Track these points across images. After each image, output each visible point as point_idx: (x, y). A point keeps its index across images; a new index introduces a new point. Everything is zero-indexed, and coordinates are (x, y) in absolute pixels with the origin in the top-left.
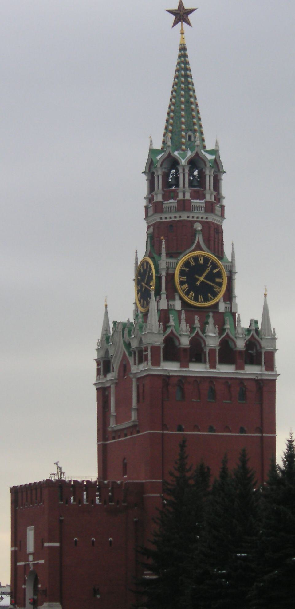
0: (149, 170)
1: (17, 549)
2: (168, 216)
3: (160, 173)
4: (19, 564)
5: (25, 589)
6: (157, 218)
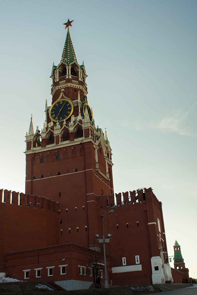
0: (59, 68)
2: (74, 85)
3: (70, 68)
6: (69, 85)
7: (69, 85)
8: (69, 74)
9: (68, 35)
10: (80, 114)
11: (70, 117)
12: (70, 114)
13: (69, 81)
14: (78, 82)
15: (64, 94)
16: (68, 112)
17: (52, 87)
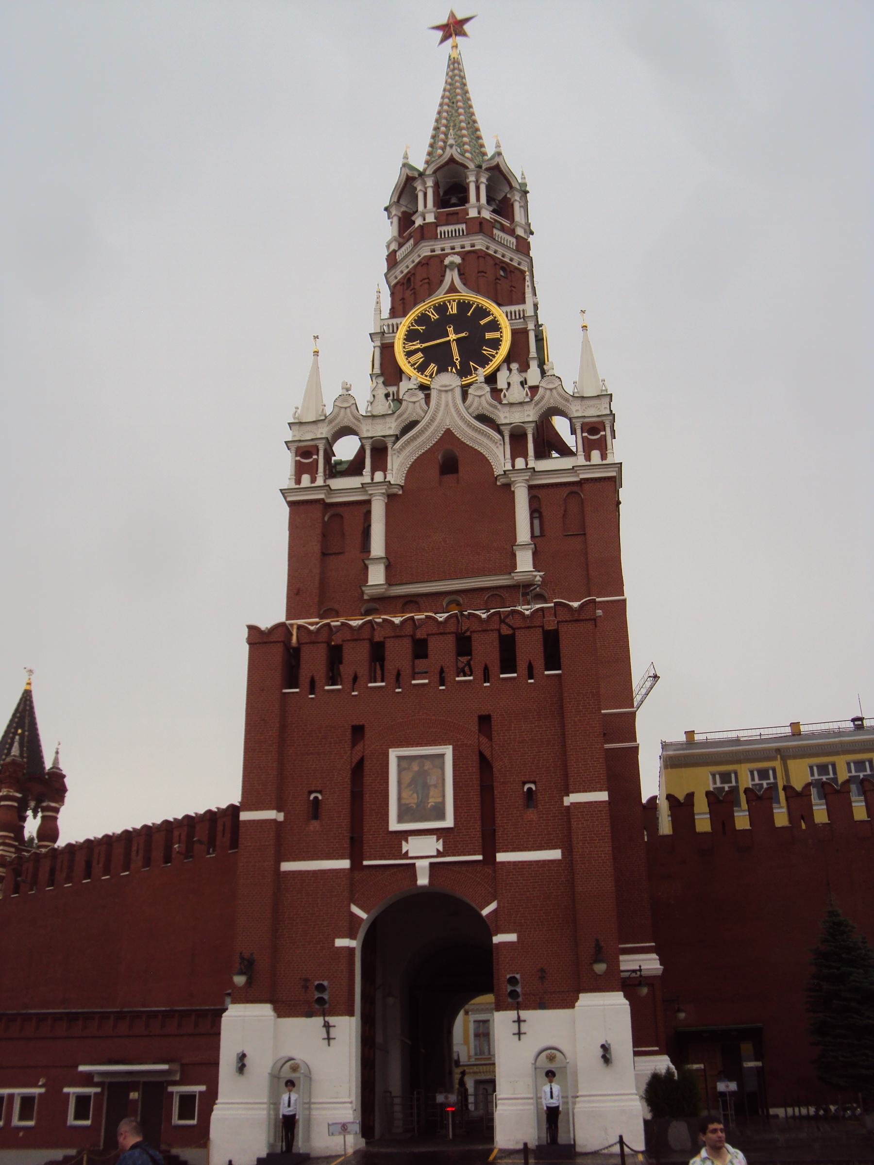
0: (435, 172)
1: (280, 817)
2: (501, 250)
3: (483, 180)
4: (287, 866)
5: (351, 951)
6: (480, 243)
7: (480, 243)
8: (478, 199)
9: (455, 65)
10: (534, 365)
11: (498, 369)
12: (494, 357)
13: (481, 227)
14: (514, 240)
15: (461, 274)
16: (487, 351)
17: (394, 246)
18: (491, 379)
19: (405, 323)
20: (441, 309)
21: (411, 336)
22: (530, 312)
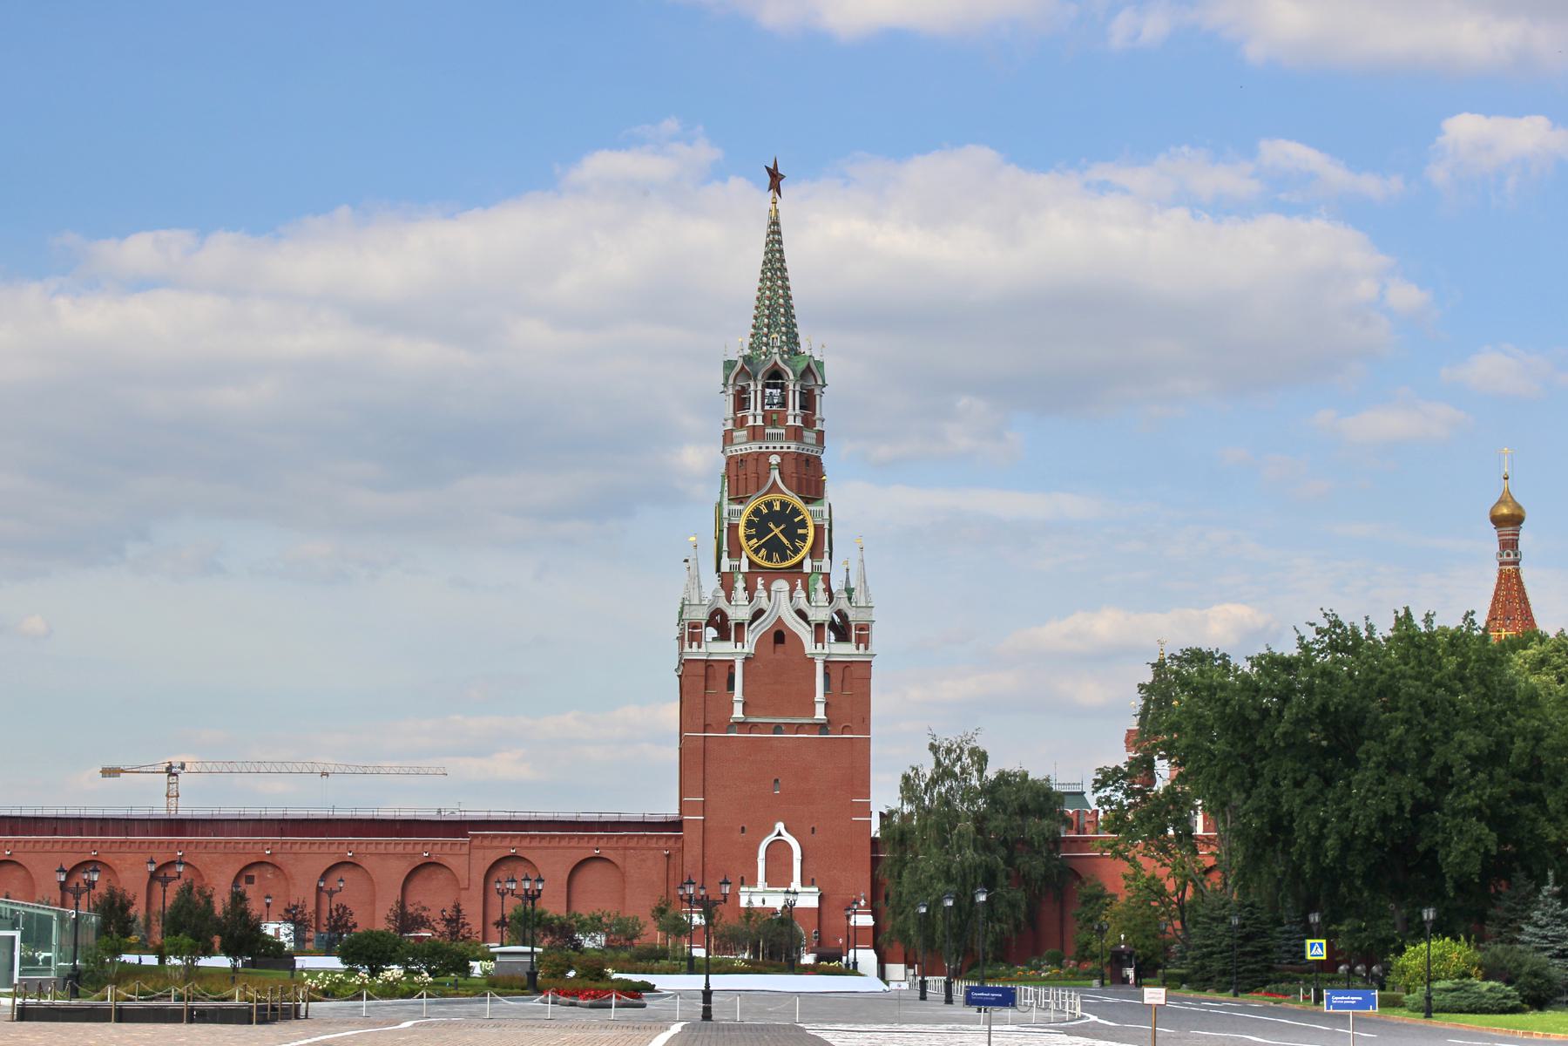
10: (826, 555)
13: (796, 434)
16: (798, 544)
18: (800, 564)
19: (747, 509)
20: (769, 505)
21: (749, 524)
22: (826, 516)
